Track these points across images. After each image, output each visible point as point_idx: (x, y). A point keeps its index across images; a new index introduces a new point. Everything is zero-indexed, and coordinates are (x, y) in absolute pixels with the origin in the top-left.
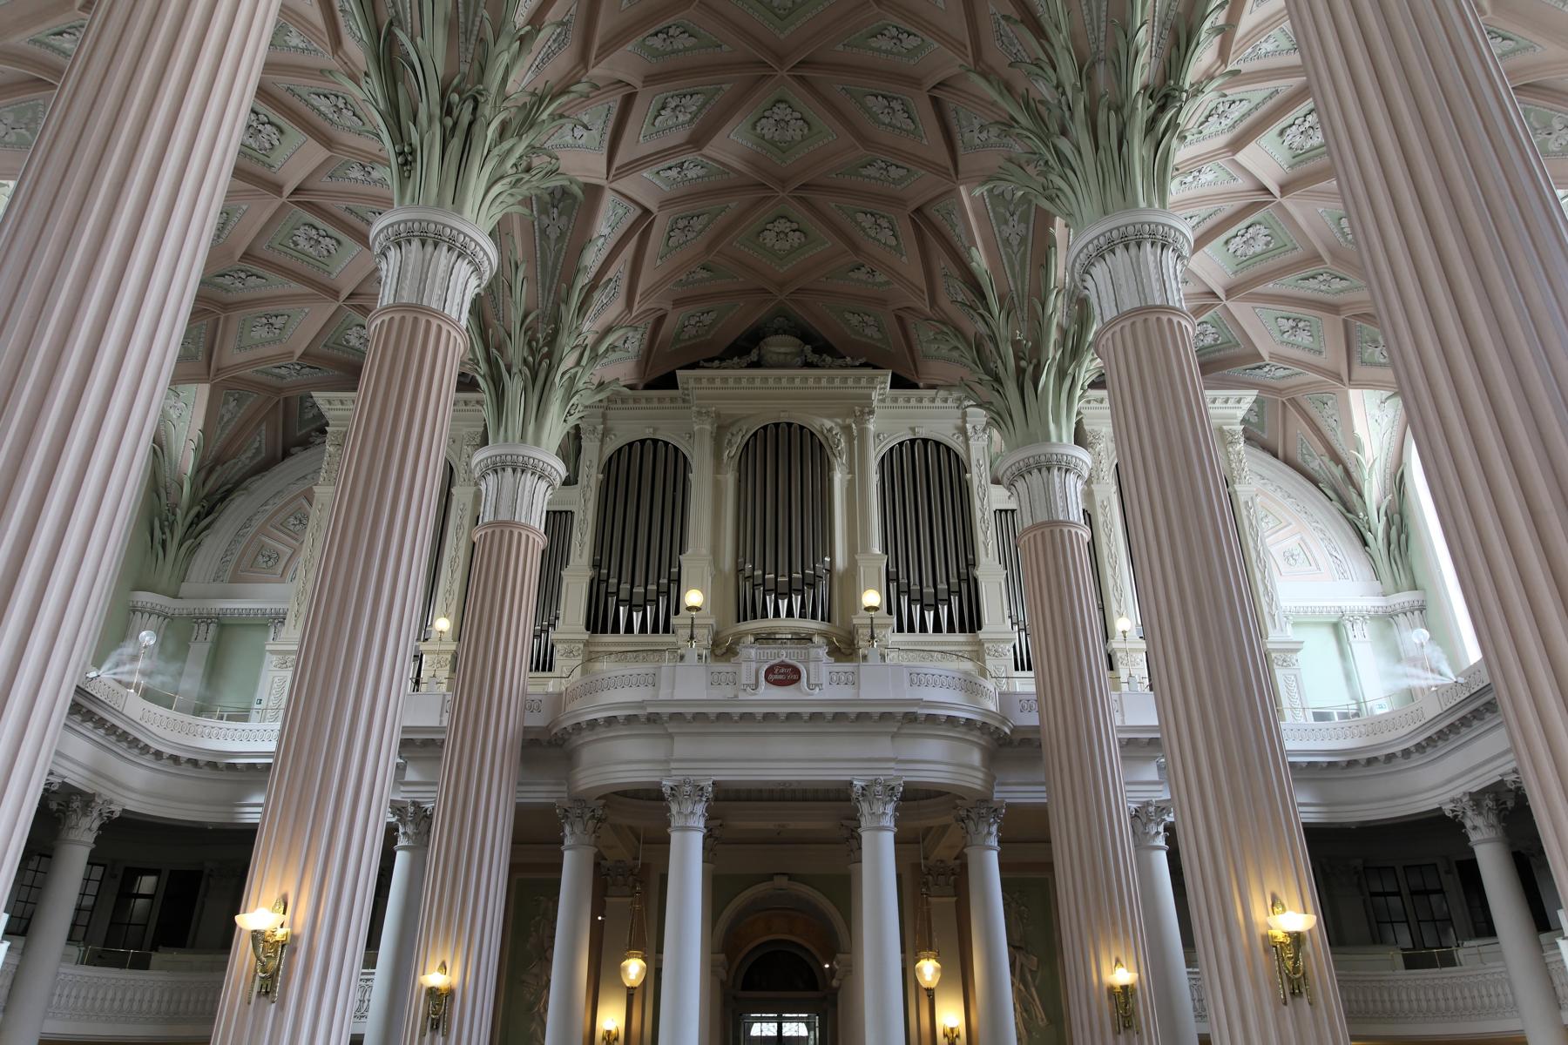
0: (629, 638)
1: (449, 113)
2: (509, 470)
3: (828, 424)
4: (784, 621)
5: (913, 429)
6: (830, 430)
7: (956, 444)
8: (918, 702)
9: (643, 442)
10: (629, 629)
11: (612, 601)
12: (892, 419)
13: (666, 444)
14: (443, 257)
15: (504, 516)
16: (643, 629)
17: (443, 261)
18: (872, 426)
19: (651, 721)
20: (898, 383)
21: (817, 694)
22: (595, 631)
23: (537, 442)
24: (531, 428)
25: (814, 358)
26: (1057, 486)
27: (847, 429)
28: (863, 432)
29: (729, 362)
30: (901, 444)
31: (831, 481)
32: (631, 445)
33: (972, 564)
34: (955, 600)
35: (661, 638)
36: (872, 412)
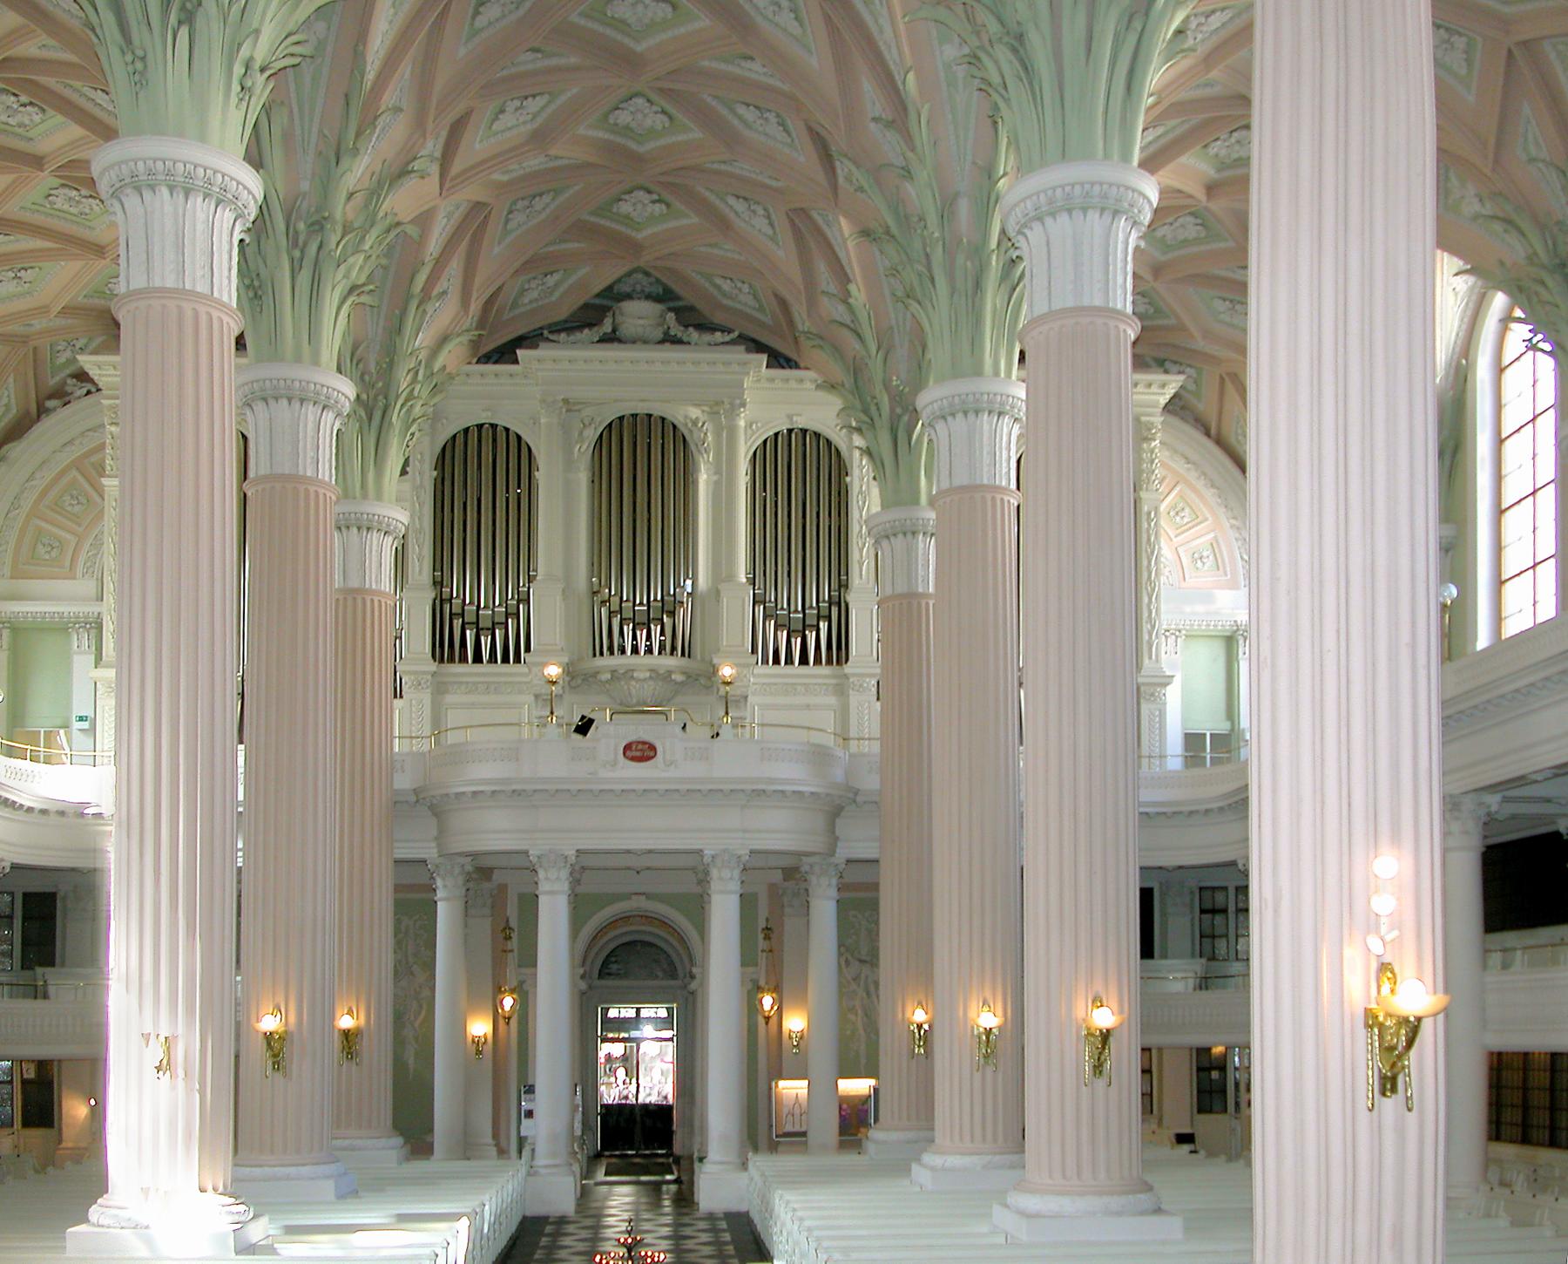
0: (478, 668)
1: (295, 244)
2: (355, 530)
3: (694, 413)
4: (642, 659)
5: (790, 417)
6: (695, 423)
7: (839, 438)
8: (771, 781)
9: (480, 427)
10: (478, 659)
11: (457, 623)
12: (768, 403)
13: (507, 430)
14: (311, 412)
15: (354, 583)
16: (493, 659)
17: (311, 417)
18: (742, 423)
19: (515, 795)
20: (779, 360)
21: (672, 773)
22: (442, 661)
23: (379, 497)
24: (371, 476)
25: (676, 330)
26: (920, 552)
27: (714, 414)
28: (732, 430)
29: (578, 336)
30: (776, 435)
31: (695, 483)
32: (466, 430)
33: (844, 586)
34: (823, 626)
35: (512, 667)
36: (743, 405)
